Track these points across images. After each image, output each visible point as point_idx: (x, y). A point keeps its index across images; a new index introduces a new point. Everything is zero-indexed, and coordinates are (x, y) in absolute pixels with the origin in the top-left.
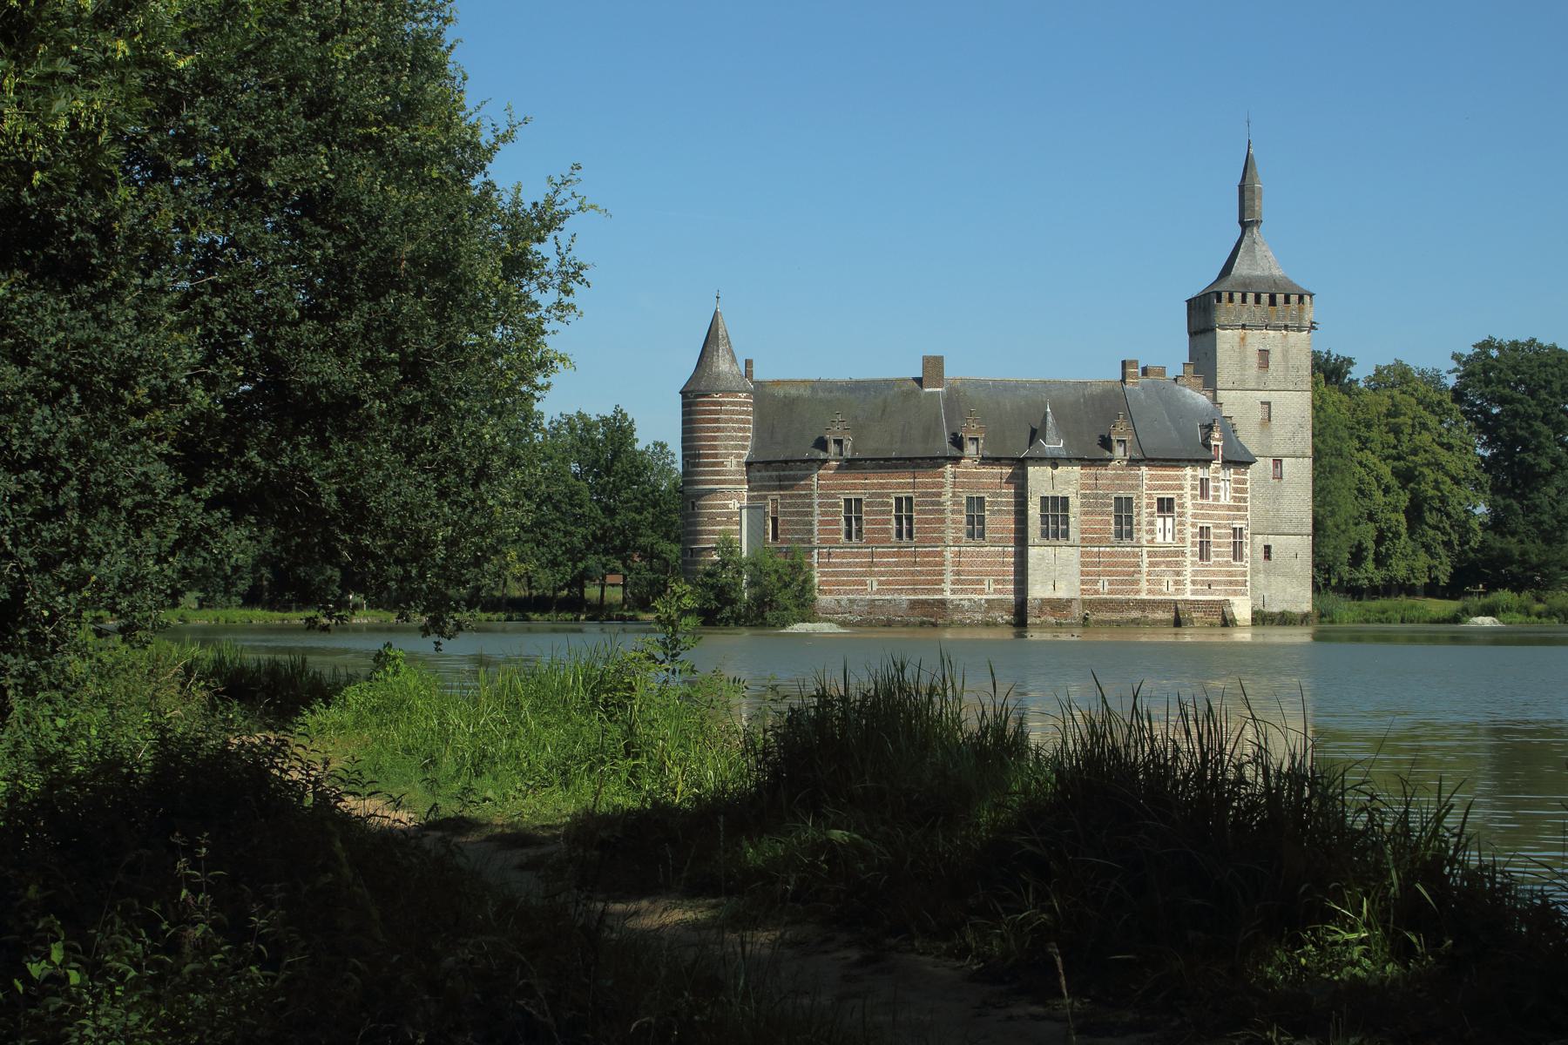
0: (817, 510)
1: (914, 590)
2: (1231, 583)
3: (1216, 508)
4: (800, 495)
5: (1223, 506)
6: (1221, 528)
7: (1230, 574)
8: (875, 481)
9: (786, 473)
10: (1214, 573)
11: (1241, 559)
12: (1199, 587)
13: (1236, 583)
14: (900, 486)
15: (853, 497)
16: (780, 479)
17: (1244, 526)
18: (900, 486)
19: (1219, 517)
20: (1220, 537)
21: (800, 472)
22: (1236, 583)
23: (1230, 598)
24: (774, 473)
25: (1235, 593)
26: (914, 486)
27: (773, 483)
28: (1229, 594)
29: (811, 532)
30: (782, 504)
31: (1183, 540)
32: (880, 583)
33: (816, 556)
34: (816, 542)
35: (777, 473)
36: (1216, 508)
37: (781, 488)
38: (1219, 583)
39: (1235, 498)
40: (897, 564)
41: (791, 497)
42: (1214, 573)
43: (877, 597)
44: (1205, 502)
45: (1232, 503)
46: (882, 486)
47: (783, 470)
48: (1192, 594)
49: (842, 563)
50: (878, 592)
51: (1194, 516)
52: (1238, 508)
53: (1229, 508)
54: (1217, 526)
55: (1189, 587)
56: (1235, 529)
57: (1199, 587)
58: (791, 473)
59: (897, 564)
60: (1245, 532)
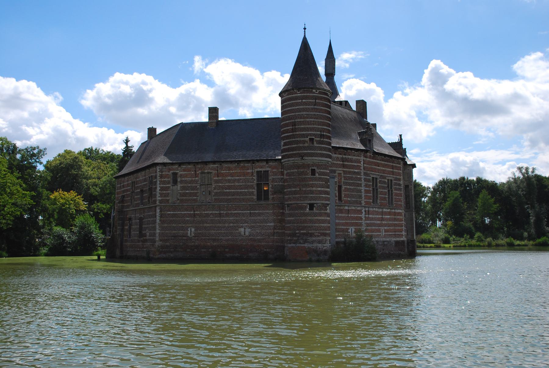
0: (363, 183)
1: (395, 235)
4: (355, 172)
8: (381, 168)
9: (346, 156)
14: (389, 173)
15: (375, 176)
16: (343, 160)
18: (389, 173)
21: (354, 157)
24: (340, 156)
26: (393, 173)
27: (339, 162)
29: (360, 197)
30: (345, 177)
32: (386, 231)
33: (364, 213)
34: (363, 204)
35: (342, 156)
37: (344, 166)
40: (390, 219)
41: (350, 173)
43: (384, 239)
46: (384, 172)
47: (345, 155)
49: (373, 218)
50: (385, 236)
58: (350, 157)
59: (390, 219)
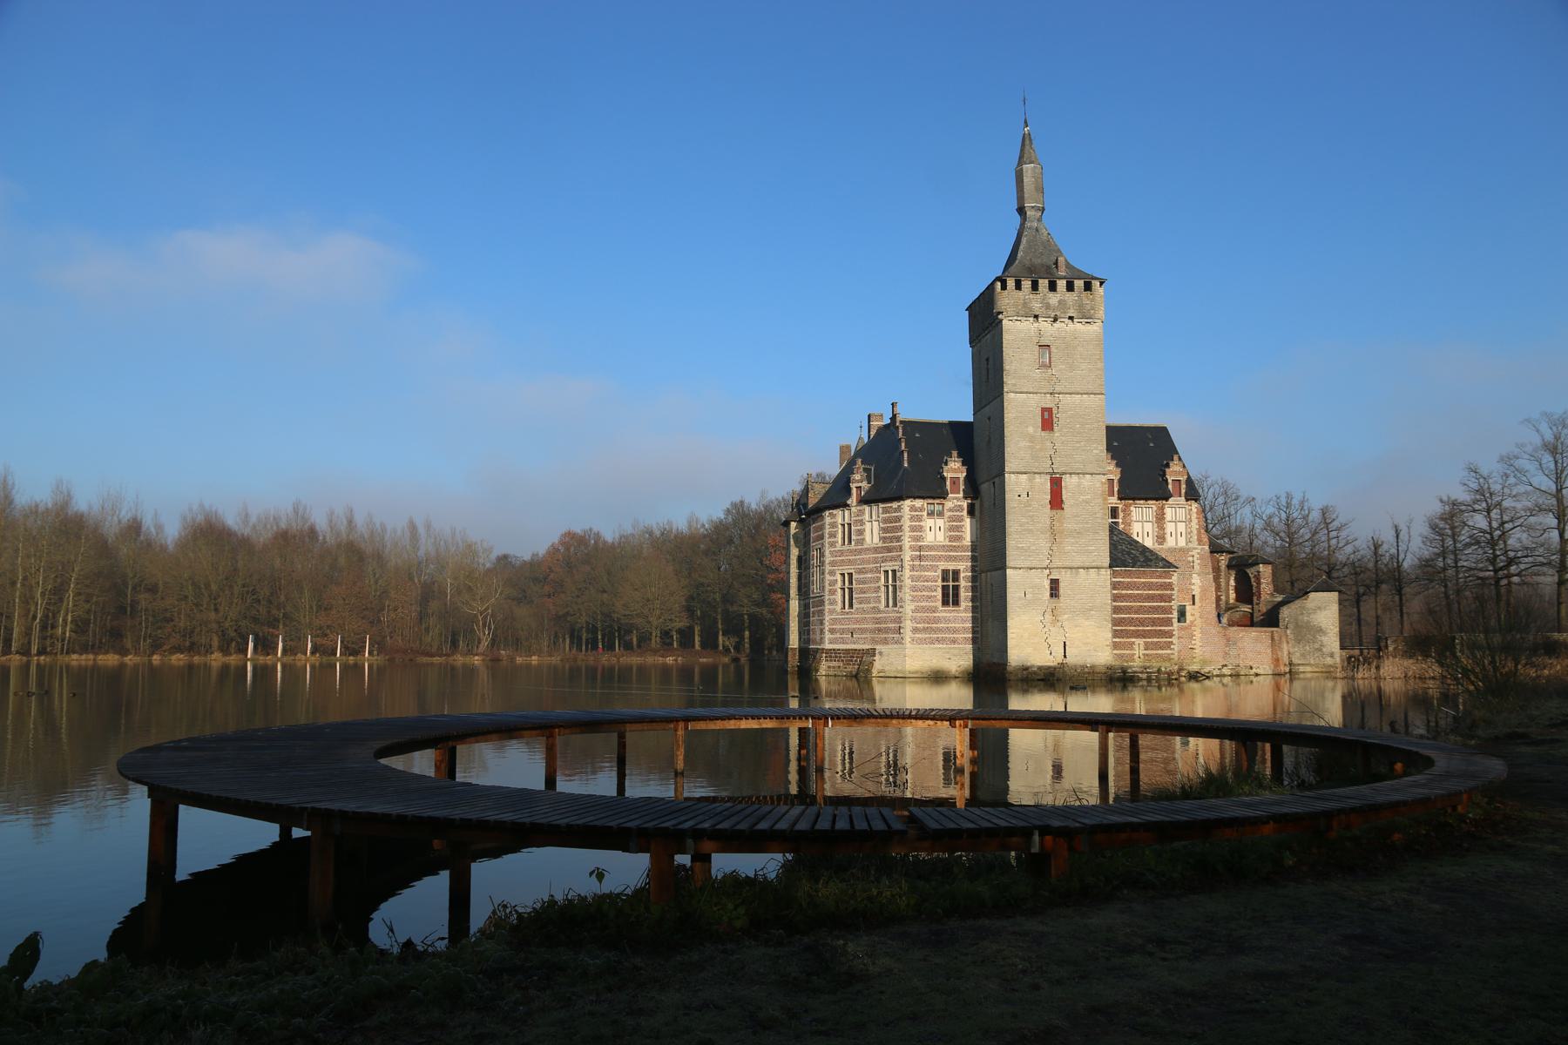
2: (879, 630)
3: (860, 552)
5: (868, 549)
6: (866, 573)
7: (878, 621)
10: (857, 621)
11: (895, 605)
12: (838, 635)
13: (887, 630)
17: (897, 568)
19: (863, 561)
20: (864, 583)
22: (887, 630)
23: (877, 647)
25: (885, 642)
28: (877, 642)
31: (823, 590)
36: (860, 552)
38: (863, 631)
39: (883, 539)
42: (857, 621)
44: (846, 547)
45: (880, 545)
48: (831, 643)
51: (833, 564)
52: (889, 550)
53: (876, 550)
54: (860, 572)
55: (827, 636)
56: (887, 572)
57: (838, 635)
60: (898, 574)
